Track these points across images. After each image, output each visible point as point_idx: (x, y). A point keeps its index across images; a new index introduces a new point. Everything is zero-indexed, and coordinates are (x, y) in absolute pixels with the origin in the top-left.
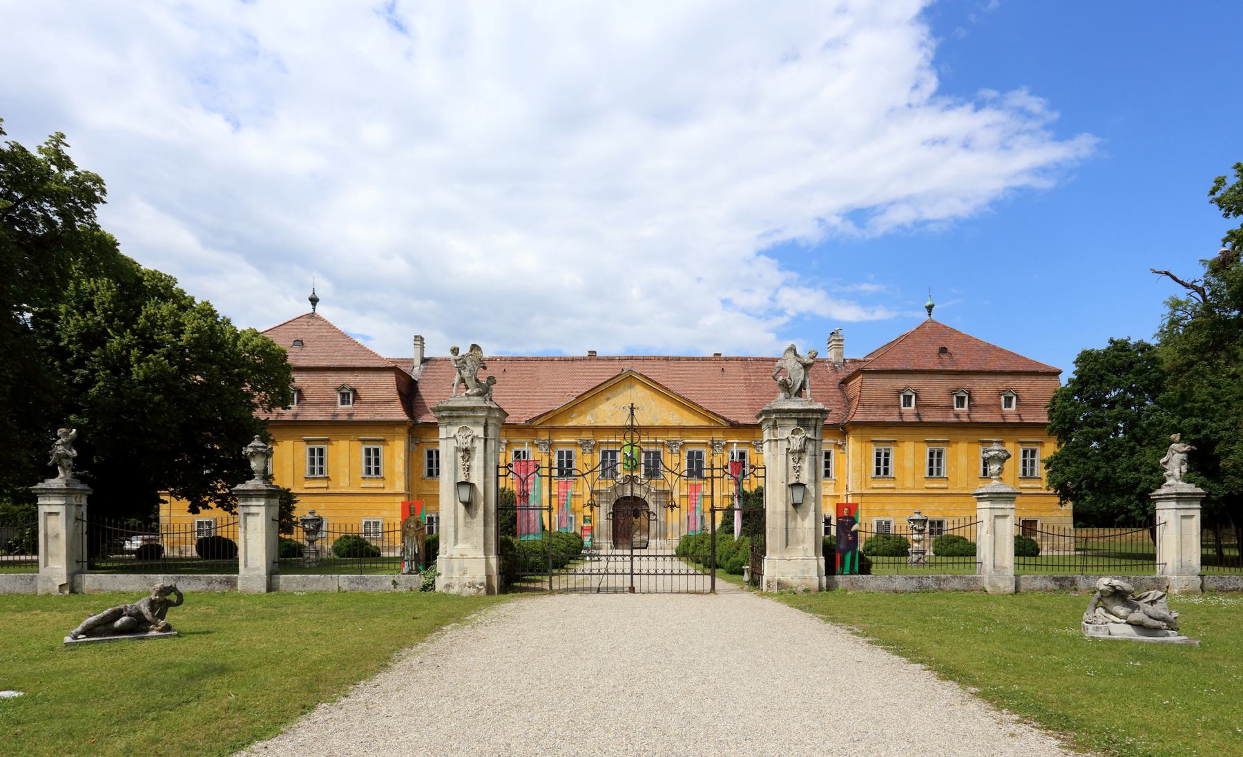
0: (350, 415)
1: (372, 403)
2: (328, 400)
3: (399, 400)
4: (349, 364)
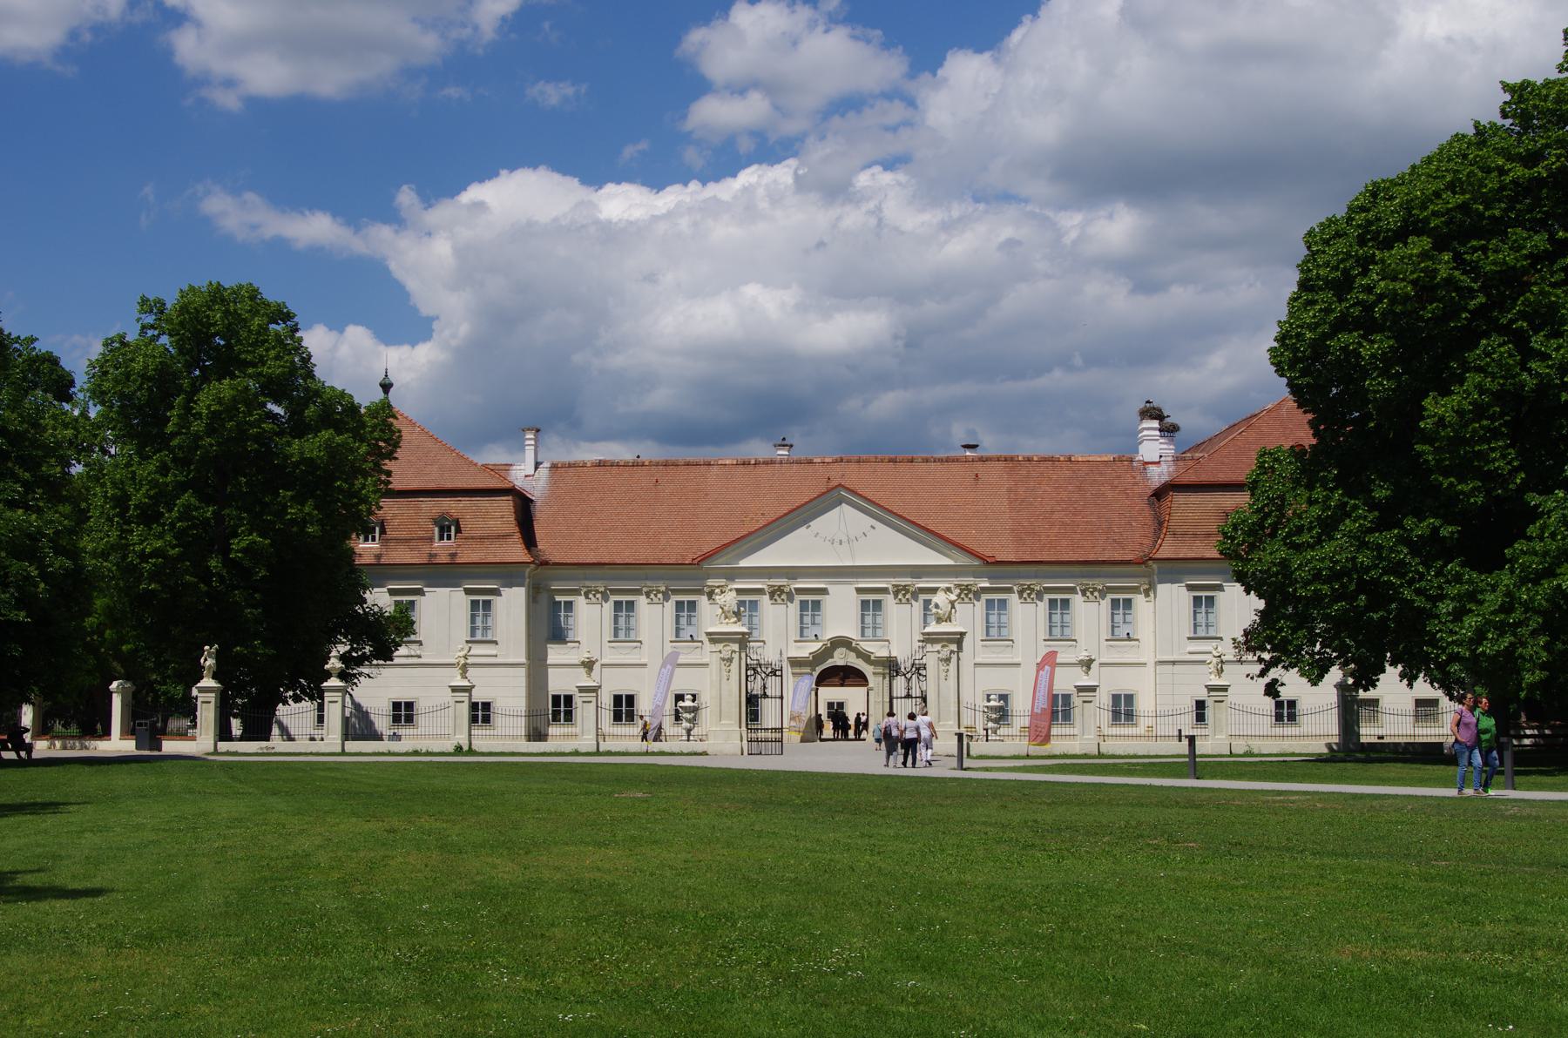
0: (453, 555)
1: (482, 538)
2: (421, 534)
3: (519, 534)
4: (449, 485)
